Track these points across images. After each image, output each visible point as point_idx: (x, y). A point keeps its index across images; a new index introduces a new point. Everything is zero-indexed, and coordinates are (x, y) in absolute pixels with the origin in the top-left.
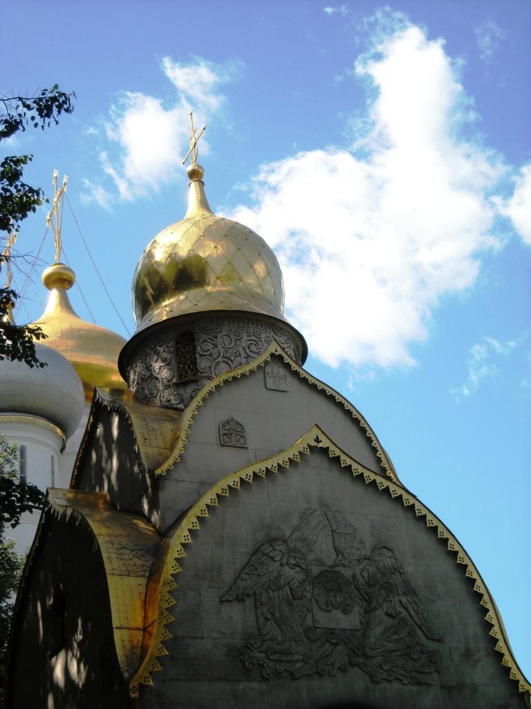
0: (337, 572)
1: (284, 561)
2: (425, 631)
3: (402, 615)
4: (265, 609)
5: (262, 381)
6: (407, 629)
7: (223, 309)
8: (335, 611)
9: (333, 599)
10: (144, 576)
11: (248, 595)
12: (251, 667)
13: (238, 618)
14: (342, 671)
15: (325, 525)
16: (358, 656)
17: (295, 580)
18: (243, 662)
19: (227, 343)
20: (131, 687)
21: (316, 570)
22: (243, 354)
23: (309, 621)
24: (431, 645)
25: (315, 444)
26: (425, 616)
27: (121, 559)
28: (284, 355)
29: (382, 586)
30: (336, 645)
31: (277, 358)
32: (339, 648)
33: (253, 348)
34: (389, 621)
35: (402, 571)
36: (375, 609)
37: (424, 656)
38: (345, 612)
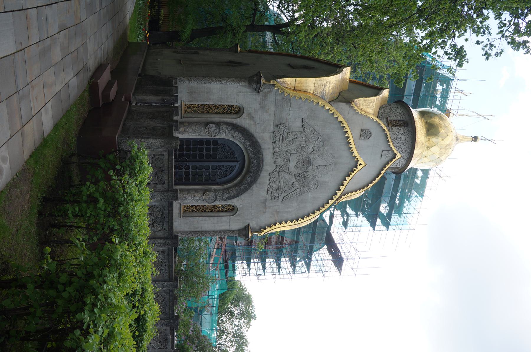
0: (310, 166)
1: (316, 145)
2: (286, 197)
3: (293, 189)
4: (299, 135)
6: (287, 189)
7: (417, 139)
8: (296, 162)
9: (300, 162)
10: (314, 92)
11: (304, 129)
12: (278, 127)
14: (274, 162)
15: (328, 163)
16: (279, 169)
17: (309, 149)
18: (280, 124)
19: (402, 139)
20: (274, 81)
21: (311, 157)
23: (293, 152)
24: (281, 198)
25: (359, 163)
26: (292, 198)
27: (321, 85)
28: (396, 159)
29: (304, 182)
30: (284, 161)
31: (394, 156)
32: (283, 162)
33: (400, 149)
34: (291, 184)
35: (309, 191)
36: (296, 178)
37: (277, 195)
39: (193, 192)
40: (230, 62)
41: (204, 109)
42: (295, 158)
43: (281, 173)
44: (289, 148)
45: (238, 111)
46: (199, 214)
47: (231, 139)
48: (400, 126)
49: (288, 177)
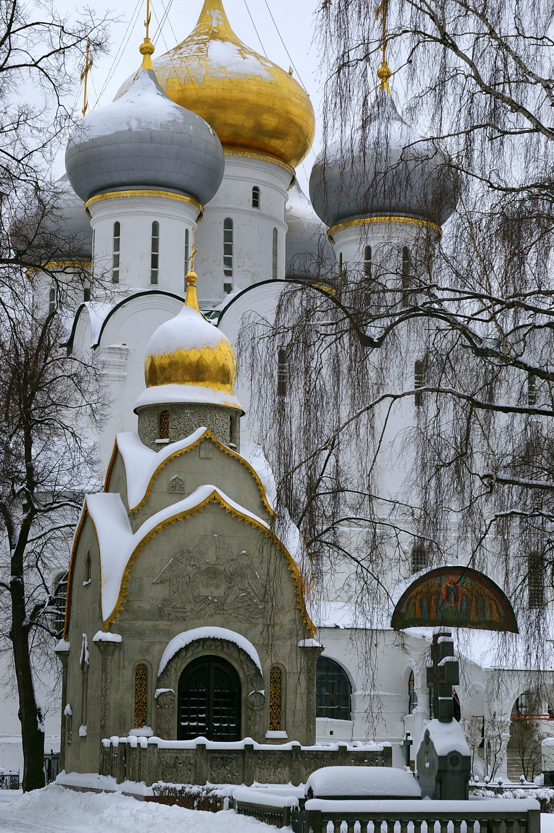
0: (215, 568)
1: (188, 563)
5: (198, 454)
21: (204, 567)
23: (196, 593)
30: (209, 604)
35: (252, 567)
36: (233, 586)
38: (217, 587)
43: (226, 607)
46: (283, 715)
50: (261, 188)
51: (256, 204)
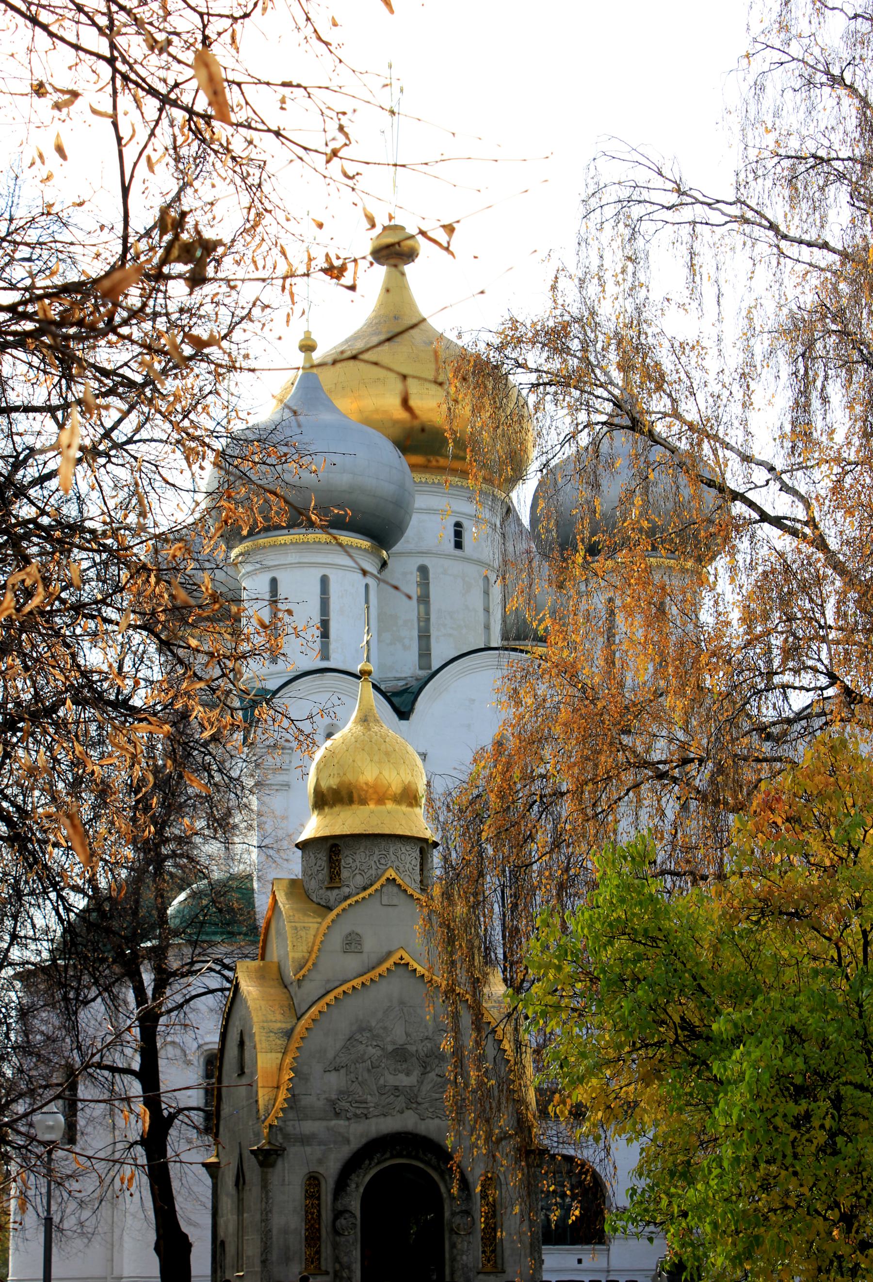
4: (352, 1075)
13: (335, 1081)
21: (390, 1048)
22: (374, 867)
23: (382, 1082)
33: (383, 861)
34: (439, 1079)
38: (408, 1075)
39: (455, 1251)
40: (237, 1184)
41: (313, 1237)
42: (391, 1077)
43: (419, 1100)
44: (375, 1088)
45: (313, 1181)
47: (361, 1190)
48: (339, 861)
49: (426, 1087)
50: (466, 523)
51: (458, 545)
